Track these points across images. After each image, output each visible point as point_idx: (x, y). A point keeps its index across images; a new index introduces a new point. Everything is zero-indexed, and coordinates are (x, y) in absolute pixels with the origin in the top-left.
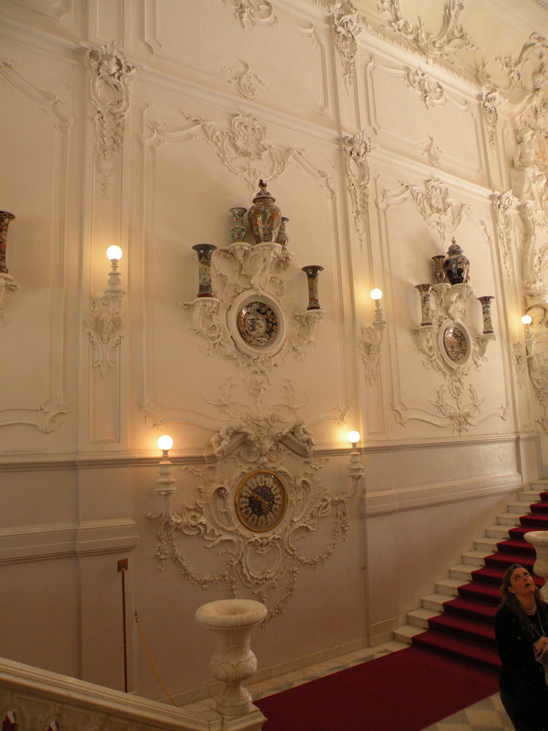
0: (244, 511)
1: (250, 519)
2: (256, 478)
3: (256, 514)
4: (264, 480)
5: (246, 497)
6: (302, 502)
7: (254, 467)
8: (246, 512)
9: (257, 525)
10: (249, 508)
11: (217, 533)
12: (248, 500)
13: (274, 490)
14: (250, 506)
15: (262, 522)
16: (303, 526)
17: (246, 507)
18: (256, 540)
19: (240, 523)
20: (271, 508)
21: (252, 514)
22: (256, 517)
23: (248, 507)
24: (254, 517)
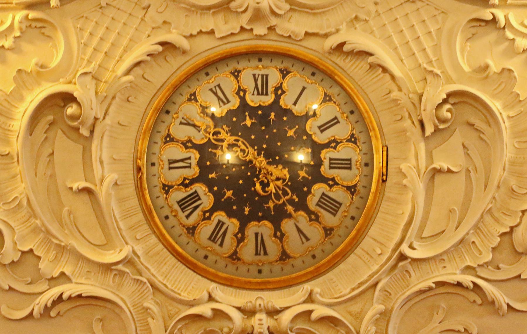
0: (180, 194)
1: (206, 230)
2: (236, 74)
3: (230, 214)
4: (272, 83)
5: (188, 144)
6: (459, 183)
7: (223, 25)
8: (189, 202)
9: (234, 257)
10: (200, 188)
11: (48, 267)
12: (195, 156)
13: (322, 128)
14: (201, 178)
15: (261, 247)
16: (459, 285)
17: (185, 184)
18: (218, 314)
19: (154, 239)
20: (304, 196)
21: (212, 211)
22: (232, 225)
23: (193, 181)
24: (220, 224)
